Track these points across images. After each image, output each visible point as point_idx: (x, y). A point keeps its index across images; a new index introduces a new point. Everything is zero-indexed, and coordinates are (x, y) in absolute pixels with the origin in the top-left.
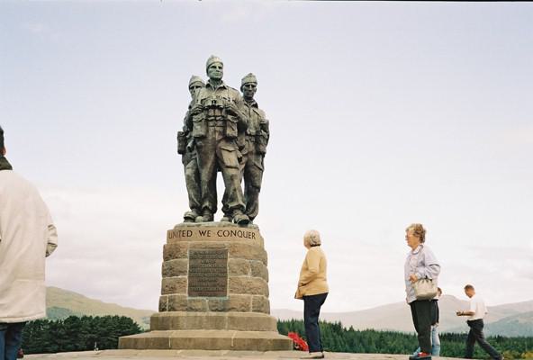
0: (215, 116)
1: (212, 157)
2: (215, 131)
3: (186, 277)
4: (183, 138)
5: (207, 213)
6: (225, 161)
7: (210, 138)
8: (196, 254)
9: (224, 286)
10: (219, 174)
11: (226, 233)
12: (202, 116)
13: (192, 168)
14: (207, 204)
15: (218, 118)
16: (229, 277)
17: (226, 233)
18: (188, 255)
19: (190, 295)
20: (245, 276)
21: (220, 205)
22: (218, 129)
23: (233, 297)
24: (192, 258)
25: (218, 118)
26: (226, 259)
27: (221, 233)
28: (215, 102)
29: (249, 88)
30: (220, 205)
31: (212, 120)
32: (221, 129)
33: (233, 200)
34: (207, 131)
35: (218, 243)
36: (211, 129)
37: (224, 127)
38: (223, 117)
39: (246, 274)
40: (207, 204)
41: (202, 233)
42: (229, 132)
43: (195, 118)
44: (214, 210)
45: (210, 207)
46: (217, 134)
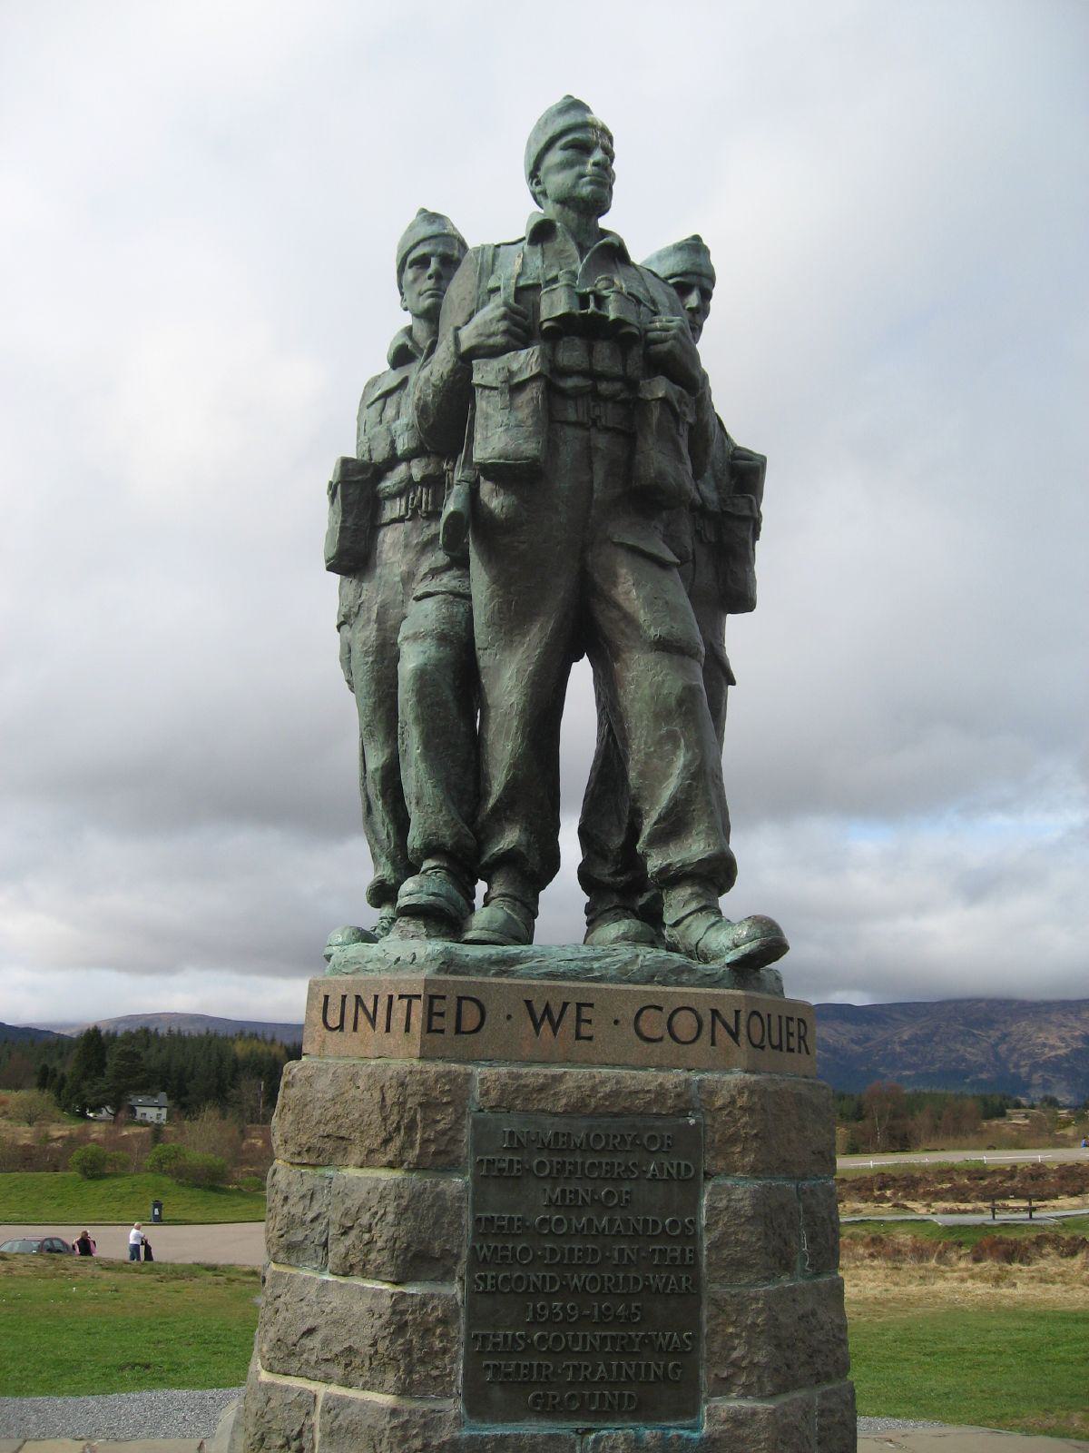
2: (589, 451)
3: (455, 1290)
4: (359, 490)
7: (563, 484)
8: (517, 1144)
9: (685, 1354)
10: (582, 674)
11: (685, 1024)
12: (526, 361)
13: (442, 638)
15: (604, 387)
16: (713, 1289)
17: (685, 1024)
18: (464, 1150)
19: (477, 1405)
20: (786, 1282)
22: (601, 441)
23: (737, 1420)
24: (491, 1175)
26: (690, 1184)
27: (654, 1024)
28: (600, 301)
31: (577, 394)
35: (650, 1078)
36: (571, 442)
37: (629, 437)
38: (632, 385)
39: (787, 1267)
41: (544, 1016)
43: (486, 372)
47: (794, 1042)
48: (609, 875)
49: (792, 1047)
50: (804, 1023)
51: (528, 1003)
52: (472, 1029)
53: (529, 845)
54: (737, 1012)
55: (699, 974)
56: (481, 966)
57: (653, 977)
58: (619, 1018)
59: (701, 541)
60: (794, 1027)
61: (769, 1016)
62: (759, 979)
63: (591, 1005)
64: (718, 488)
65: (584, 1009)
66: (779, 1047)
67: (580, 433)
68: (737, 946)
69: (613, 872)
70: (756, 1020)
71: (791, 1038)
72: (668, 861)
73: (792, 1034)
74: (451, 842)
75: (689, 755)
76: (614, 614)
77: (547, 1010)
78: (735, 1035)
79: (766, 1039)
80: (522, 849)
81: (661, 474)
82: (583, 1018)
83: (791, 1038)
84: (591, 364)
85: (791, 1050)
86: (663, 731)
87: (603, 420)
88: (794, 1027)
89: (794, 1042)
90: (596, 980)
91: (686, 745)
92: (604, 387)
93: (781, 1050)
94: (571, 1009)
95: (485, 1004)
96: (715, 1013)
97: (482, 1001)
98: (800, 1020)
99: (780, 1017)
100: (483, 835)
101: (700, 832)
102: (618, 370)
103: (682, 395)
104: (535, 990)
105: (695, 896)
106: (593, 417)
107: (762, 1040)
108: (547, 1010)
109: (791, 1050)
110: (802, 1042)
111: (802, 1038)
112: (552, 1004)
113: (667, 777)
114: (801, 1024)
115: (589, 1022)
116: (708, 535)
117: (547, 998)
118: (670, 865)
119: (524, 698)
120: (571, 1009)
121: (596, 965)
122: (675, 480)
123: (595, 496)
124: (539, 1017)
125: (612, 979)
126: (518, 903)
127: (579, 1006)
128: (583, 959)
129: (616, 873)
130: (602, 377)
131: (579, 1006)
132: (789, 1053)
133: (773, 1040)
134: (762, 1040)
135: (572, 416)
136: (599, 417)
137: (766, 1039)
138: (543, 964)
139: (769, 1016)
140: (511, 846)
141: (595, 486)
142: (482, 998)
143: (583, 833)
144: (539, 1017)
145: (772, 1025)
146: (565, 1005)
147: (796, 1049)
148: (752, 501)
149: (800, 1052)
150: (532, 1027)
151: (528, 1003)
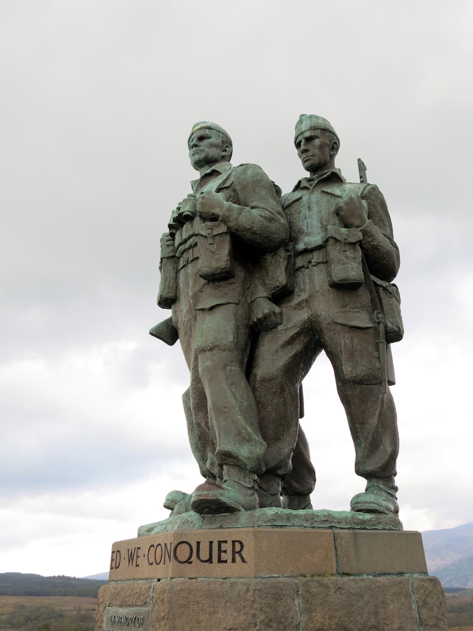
25: (187, 245)
29: (318, 145)
47: (227, 556)
50: (241, 543)
60: (228, 547)
61: (198, 543)
66: (210, 560)
78: (169, 557)
85: (226, 562)
88: (228, 547)
89: (227, 556)
93: (212, 562)
98: (234, 542)
99: (211, 543)
107: (190, 558)
110: (237, 556)
111: (234, 552)
122: (209, 267)
132: (221, 564)
134: (190, 558)
139: (198, 543)
147: (230, 560)
149: (234, 560)
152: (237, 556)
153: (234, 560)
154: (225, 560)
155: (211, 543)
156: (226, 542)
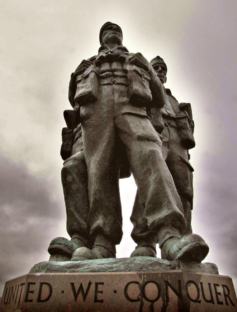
0: (113, 71)
1: (107, 133)
2: (113, 91)
5: (99, 241)
6: (134, 130)
7: (104, 100)
14: (99, 221)
21: (128, 227)
22: (116, 87)
30: (128, 227)
32: (123, 88)
33: (156, 205)
34: (99, 91)
40: (99, 221)
42: (136, 87)
44: (117, 237)
45: (107, 229)
46: (116, 95)
48: (140, 233)
49: (221, 301)
51: (72, 284)
52: (45, 299)
53: (104, 223)
54: (179, 282)
55: (164, 266)
56: (62, 269)
57: (142, 268)
58: (117, 289)
59: (171, 127)
62: (200, 267)
63: (102, 283)
64: (175, 112)
65: (99, 286)
67: (110, 87)
68: (180, 249)
69: (141, 231)
70: (193, 286)
71: (219, 296)
72: (154, 220)
73: (218, 294)
74: (78, 227)
75: (155, 175)
76: (126, 136)
77: (81, 287)
79: (201, 298)
80: (101, 225)
81: (136, 90)
82: (98, 290)
83: (219, 296)
84: (111, 68)
86: (145, 169)
87: (117, 82)
90: (116, 271)
91: (154, 172)
92: (116, 73)
93: (213, 303)
94: (93, 287)
95: (52, 286)
96: (167, 282)
97: (51, 284)
99: (209, 284)
100: (89, 223)
101: (165, 205)
102: (120, 68)
103: (142, 70)
104: (76, 277)
105: (168, 233)
106: (113, 81)
108: (81, 287)
109: (222, 303)
110: (227, 298)
111: (225, 296)
112: (83, 284)
113: (149, 187)
114: (225, 288)
115: (102, 292)
116: (173, 124)
117: (81, 281)
118: (154, 221)
119: (96, 169)
120: (93, 287)
121: (115, 265)
122: (142, 92)
123: (115, 102)
124: (77, 291)
125: (121, 271)
126: (103, 248)
127: (97, 284)
128: (109, 263)
129: (142, 232)
130: (115, 70)
131: (97, 284)
133: (206, 296)
135: (106, 82)
136: (115, 81)
137: (201, 298)
138: (90, 267)
140: (97, 225)
141: (115, 99)
142: (51, 282)
143: (132, 219)
144: (77, 291)
145: (204, 288)
146: (90, 284)
148: (185, 112)
150: (73, 297)
151: (72, 284)
152: (227, 298)
153: (227, 304)
154: (221, 301)
155: (209, 284)
156: (218, 285)
